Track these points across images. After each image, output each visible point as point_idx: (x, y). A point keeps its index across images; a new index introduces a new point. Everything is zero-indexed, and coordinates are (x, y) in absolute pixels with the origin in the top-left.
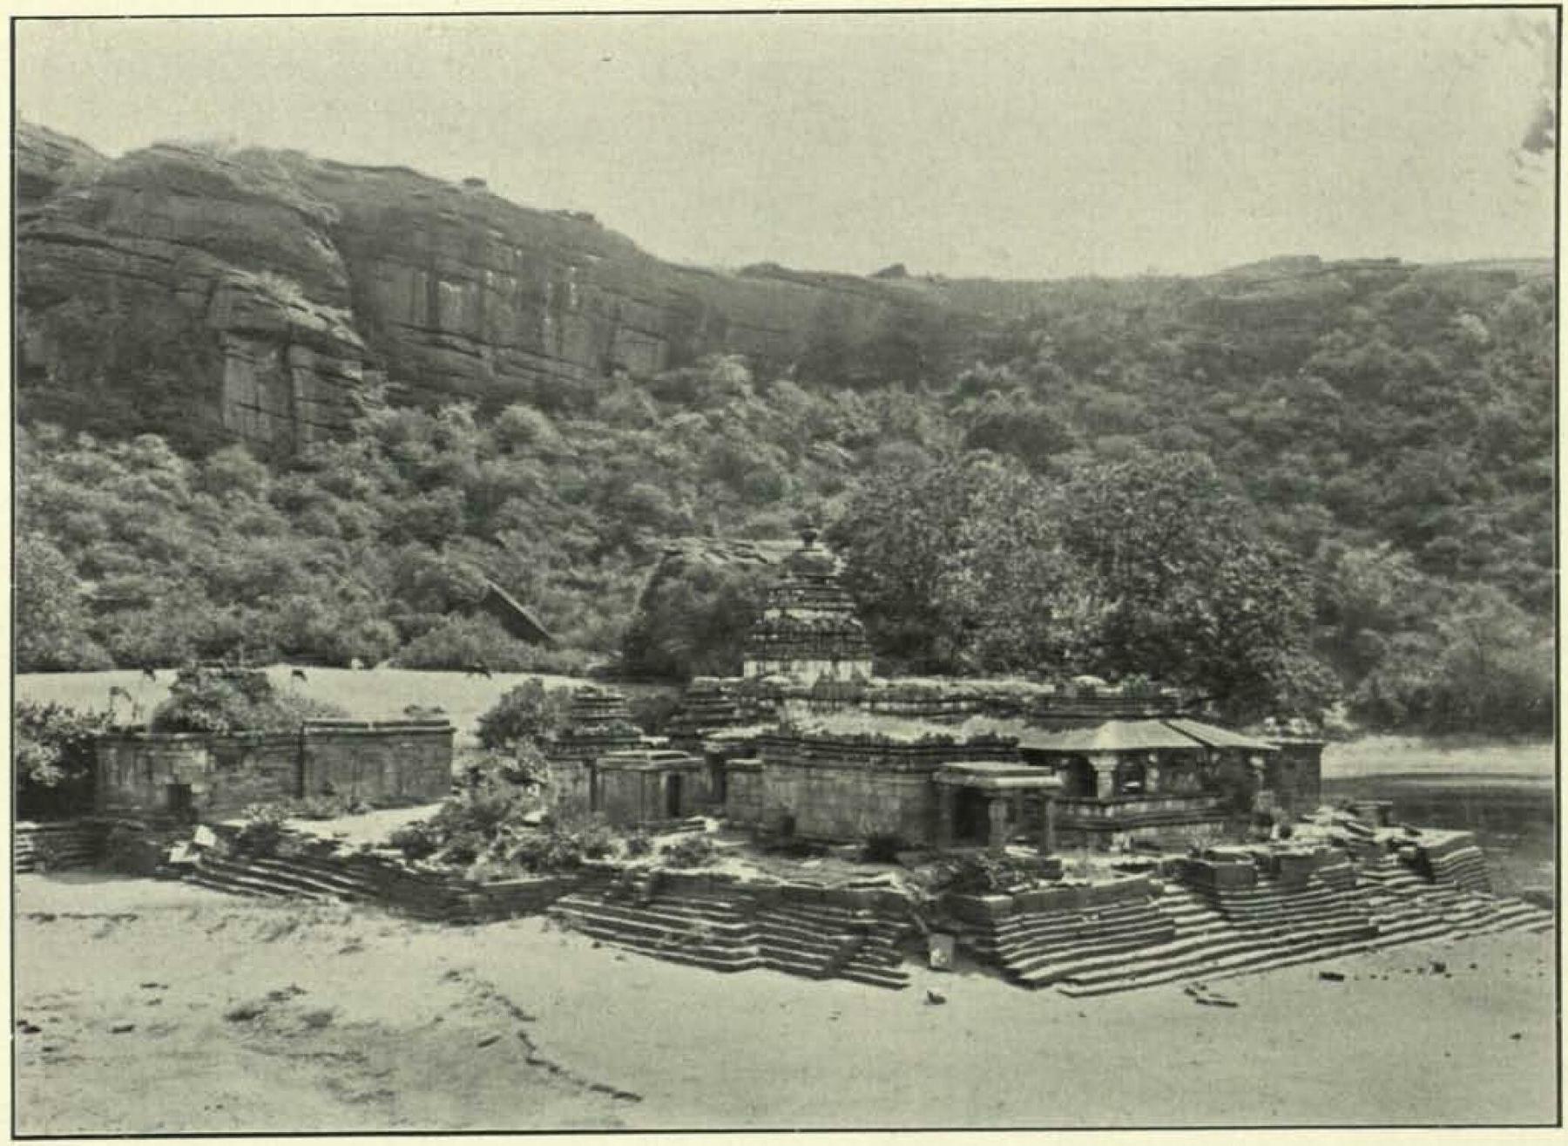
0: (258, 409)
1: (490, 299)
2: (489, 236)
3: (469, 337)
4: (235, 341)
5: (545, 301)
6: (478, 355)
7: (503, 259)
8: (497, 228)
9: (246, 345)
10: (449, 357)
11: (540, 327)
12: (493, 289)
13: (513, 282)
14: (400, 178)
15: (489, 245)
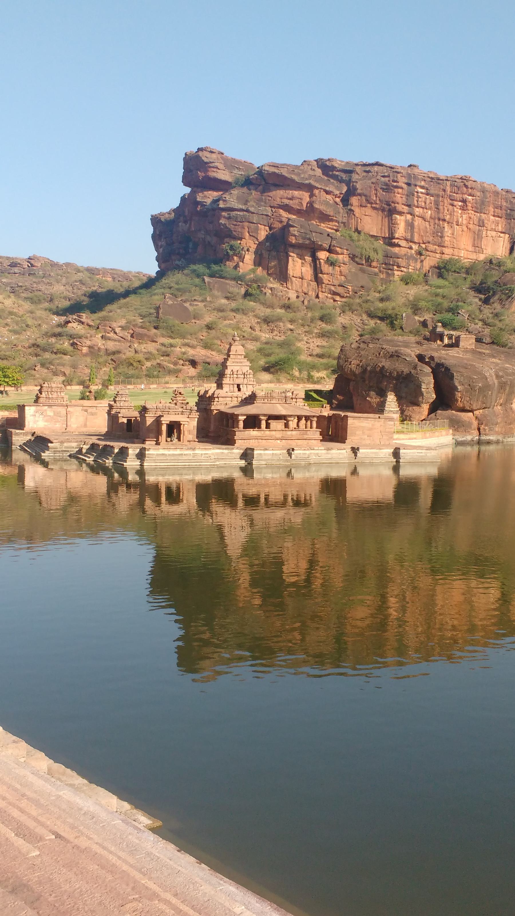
0: (302, 278)
1: (418, 222)
2: (417, 192)
3: (406, 240)
4: (291, 249)
5: (444, 220)
6: (411, 248)
7: (425, 203)
8: (422, 187)
9: (297, 251)
10: (396, 250)
11: (442, 233)
12: (419, 217)
13: (429, 212)
14: (376, 168)
15: (418, 197)
